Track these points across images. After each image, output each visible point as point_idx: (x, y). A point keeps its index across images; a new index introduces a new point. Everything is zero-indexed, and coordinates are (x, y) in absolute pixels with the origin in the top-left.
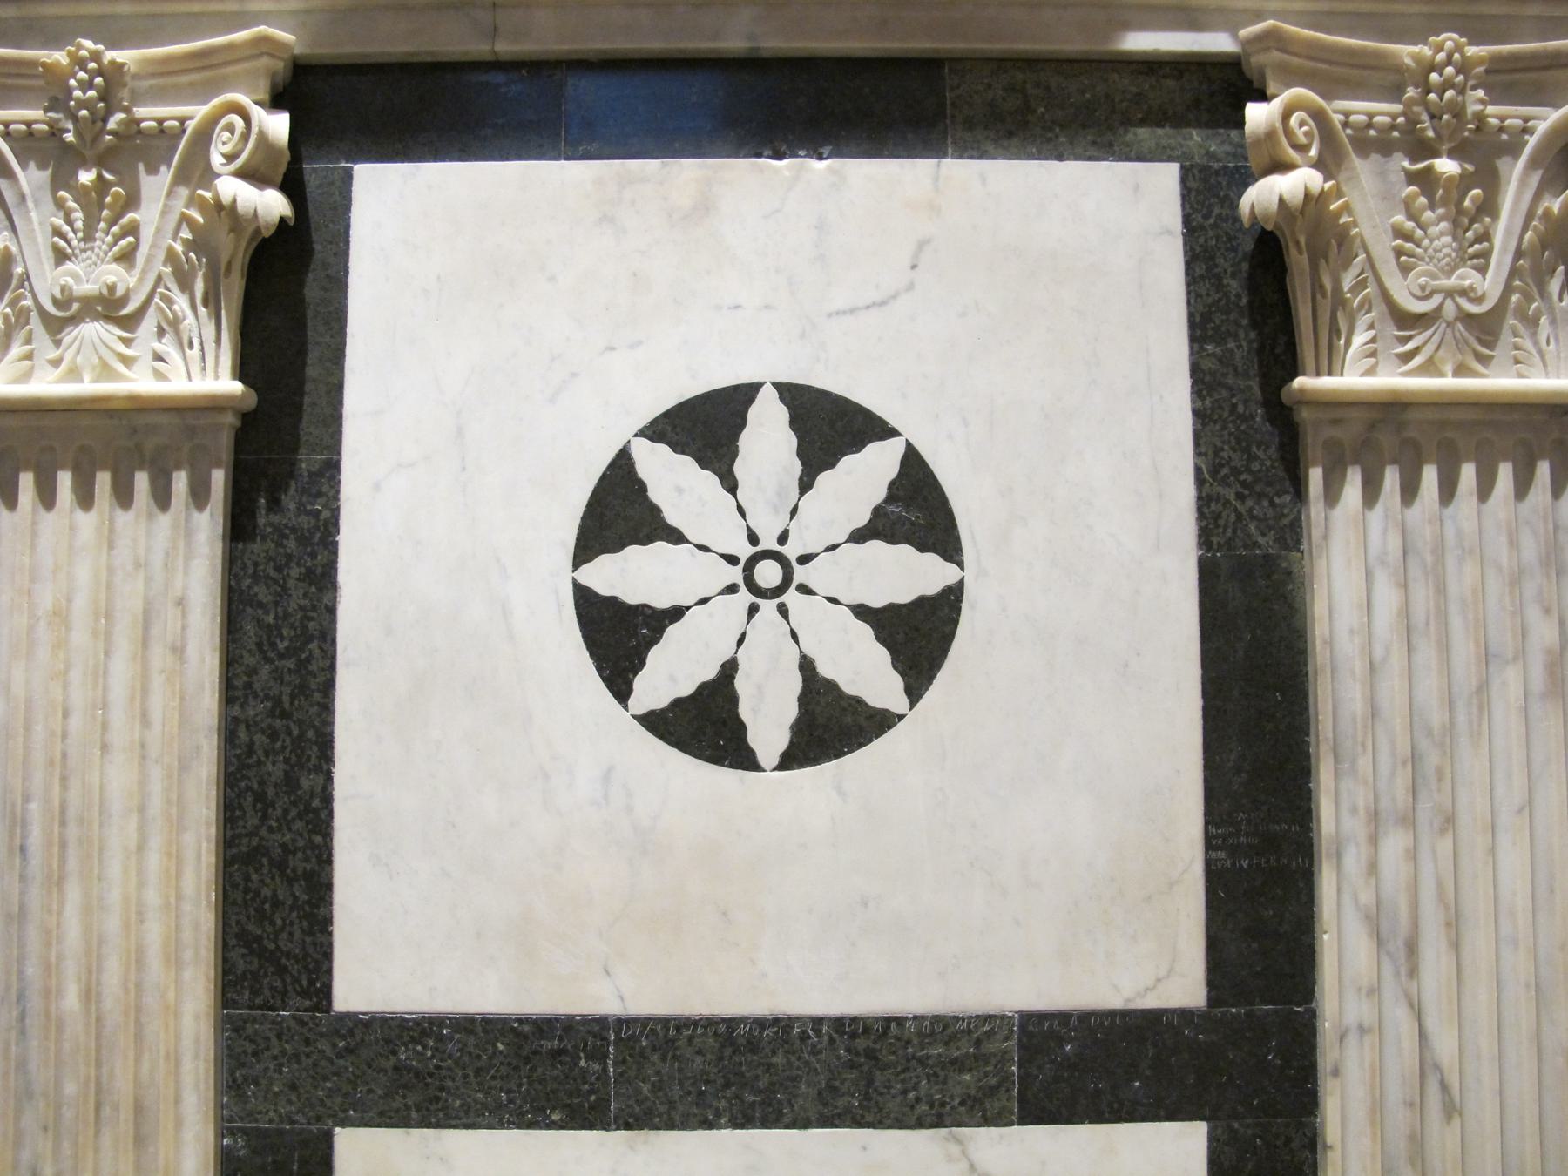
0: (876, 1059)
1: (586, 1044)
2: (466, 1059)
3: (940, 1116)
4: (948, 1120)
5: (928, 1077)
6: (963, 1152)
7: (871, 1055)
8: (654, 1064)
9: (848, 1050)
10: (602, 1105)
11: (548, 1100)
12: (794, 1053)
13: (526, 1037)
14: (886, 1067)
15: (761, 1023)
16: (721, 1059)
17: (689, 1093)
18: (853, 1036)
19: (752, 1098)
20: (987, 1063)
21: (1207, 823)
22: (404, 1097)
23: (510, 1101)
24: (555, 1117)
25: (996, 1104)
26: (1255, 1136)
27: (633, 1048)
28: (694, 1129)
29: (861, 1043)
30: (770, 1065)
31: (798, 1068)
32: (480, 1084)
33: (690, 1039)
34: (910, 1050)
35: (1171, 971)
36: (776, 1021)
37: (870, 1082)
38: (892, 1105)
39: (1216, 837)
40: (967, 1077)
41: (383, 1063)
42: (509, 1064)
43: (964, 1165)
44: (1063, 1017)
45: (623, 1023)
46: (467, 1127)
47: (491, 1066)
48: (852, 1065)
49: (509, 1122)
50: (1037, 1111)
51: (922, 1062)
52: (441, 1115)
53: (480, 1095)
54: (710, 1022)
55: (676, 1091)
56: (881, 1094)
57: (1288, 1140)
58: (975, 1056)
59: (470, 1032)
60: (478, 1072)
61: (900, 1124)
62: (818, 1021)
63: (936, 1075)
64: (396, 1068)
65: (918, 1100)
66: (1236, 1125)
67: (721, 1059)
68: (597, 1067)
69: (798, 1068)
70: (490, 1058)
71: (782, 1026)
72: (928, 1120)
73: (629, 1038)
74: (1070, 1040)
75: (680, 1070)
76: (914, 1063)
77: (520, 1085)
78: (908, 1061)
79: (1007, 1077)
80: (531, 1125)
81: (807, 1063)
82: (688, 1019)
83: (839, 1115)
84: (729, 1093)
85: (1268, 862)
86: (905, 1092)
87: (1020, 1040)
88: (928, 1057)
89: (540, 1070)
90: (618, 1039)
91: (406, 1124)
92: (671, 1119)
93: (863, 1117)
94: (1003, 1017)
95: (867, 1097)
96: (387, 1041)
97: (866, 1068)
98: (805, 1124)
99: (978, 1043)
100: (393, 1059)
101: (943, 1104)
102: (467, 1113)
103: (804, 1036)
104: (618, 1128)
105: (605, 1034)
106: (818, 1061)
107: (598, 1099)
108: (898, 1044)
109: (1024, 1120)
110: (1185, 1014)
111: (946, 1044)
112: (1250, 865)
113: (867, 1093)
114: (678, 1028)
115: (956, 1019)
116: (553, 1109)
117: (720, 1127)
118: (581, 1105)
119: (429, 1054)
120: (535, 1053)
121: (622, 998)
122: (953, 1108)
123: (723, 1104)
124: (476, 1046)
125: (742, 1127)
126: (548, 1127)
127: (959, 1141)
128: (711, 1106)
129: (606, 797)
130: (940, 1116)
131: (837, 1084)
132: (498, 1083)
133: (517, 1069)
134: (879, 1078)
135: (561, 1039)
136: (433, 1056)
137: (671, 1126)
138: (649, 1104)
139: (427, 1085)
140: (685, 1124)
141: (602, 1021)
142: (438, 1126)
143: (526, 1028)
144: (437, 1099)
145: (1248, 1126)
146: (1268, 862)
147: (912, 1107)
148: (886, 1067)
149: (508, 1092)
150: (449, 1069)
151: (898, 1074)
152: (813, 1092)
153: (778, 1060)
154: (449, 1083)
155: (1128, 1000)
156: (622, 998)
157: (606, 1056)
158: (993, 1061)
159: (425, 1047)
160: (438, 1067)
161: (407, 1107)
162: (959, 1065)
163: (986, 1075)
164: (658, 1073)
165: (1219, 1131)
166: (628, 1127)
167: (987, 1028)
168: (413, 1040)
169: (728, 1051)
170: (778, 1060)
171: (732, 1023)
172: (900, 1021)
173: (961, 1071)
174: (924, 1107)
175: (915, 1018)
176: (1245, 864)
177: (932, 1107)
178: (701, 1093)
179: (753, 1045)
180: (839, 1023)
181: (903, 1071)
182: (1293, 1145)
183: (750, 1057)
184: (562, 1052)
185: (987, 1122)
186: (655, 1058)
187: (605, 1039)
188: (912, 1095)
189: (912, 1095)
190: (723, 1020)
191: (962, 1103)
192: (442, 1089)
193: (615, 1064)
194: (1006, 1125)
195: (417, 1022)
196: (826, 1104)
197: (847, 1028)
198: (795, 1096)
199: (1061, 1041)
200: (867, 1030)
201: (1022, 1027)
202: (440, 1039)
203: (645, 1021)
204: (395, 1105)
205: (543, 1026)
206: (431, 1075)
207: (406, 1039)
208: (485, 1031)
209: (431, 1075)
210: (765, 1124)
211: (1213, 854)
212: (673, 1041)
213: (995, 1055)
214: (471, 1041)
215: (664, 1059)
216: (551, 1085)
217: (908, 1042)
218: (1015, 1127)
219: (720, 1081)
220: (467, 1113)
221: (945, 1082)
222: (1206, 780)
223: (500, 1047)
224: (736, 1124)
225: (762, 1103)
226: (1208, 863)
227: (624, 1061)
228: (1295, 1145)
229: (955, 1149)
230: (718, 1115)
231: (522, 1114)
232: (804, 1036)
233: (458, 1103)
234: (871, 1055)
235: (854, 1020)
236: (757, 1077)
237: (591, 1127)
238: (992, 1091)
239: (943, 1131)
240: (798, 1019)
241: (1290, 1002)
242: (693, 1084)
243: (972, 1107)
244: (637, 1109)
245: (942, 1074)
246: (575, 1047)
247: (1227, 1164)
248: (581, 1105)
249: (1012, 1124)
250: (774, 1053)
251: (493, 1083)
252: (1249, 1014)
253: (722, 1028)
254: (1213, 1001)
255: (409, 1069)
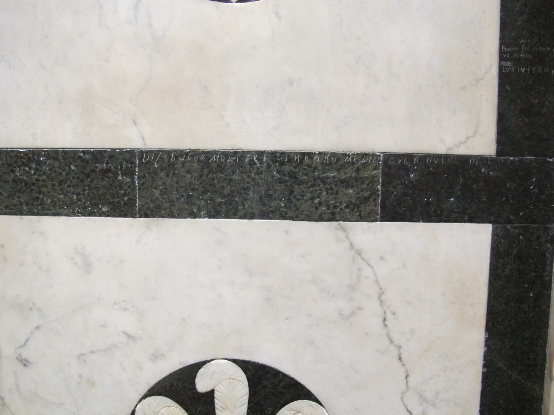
0: (296, 178)
1: (122, 166)
2: (54, 175)
3: (333, 214)
4: (338, 217)
5: (327, 189)
6: (346, 236)
7: (292, 175)
8: (162, 178)
9: (279, 172)
10: (131, 203)
11: (100, 199)
12: (246, 173)
13: (87, 162)
14: (302, 183)
15: (226, 154)
16: (201, 176)
17: (182, 196)
18: (282, 163)
19: (219, 200)
20: (363, 183)
21: (501, 45)
22: (19, 197)
23: (79, 200)
24: (104, 209)
25: (368, 208)
26: (520, 234)
27: (149, 169)
28: (185, 218)
29: (287, 168)
30: (231, 180)
31: (248, 183)
32: (61, 189)
33: (183, 163)
34: (316, 173)
35: (475, 132)
36: (235, 153)
37: (291, 192)
38: (305, 206)
39: (506, 53)
40: (351, 191)
41: (7, 178)
42: (78, 178)
43: (347, 244)
44: (410, 157)
45: (143, 153)
46: (54, 215)
47: (68, 179)
48: (281, 182)
49: (78, 212)
50: (393, 213)
51: (324, 181)
52: (40, 208)
53: (61, 196)
54: (195, 154)
55: (175, 195)
56: (298, 200)
57: (539, 237)
58: (356, 179)
59: (55, 159)
60: (61, 183)
61: (309, 218)
62: (260, 154)
63: (332, 189)
64: (14, 181)
65: (320, 204)
66: (509, 227)
67: (201, 176)
68: (128, 180)
69: (248, 183)
70: (67, 174)
71: (239, 156)
72: (327, 216)
73: (147, 163)
74: (414, 171)
75: (177, 182)
76: (318, 181)
77: (84, 190)
78: (315, 180)
79: (374, 192)
80: (91, 214)
81: (254, 179)
82: (182, 151)
83: (272, 211)
84: (206, 196)
85: (537, 70)
86: (312, 199)
87: (383, 170)
88: (327, 178)
89: (95, 181)
90: (141, 163)
91: (20, 213)
92: (172, 212)
93: (286, 213)
94: (373, 155)
95: (289, 201)
96: (9, 165)
97: (289, 183)
98: (252, 217)
99: (358, 170)
100: (12, 175)
101: (335, 207)
102: (54, 206)
103: (252, 163)
104: (140, 217)
105: (132, 160)
106: (260, 178)
107: (129, 199)
108: (309, 169)
109: (384, 219)
110: (483, 159)
111: (338, 170)
112: (526, 71)
113: (289, 199)
114: (176, 157)
115: (345, 155)
116: (103, 205)
117: (200, 217)
118: (119, 202)
119: (33, 172)
120: (92, 171)
121: (143, 139)
122: (341, 209)
123: (202, 203)
124: (59, 167)
125: (214, 217)
126: (100, 215)
127: (344, 229)
128: (195, 204)
129: (136, 18)
130: (333, 214)
131: (272, 192)
132: (72, 189)
133: (82, 181)
134: (297, 189)
135: (107, 163)
136: (35, 174)
137: (171, 215)
138: (158, 202)
139: (32, 190)
140: (180, 215)
141: (131, 152)
142: (38, 214)
143: (87, 156)
144: (38, 198)
145: (516, 228)
146: (537, 70)
147: (317, 208)
148: (302, 183)
149: (78, 194)
150: (44, 181)
151: (309, 188)
152: (257, 197)
153: (236, 177)
154: (44, 189)
155: (449, 149)
156: (143, 139)
157: (133, 173)
158: (367, 182)
159: (30, 168)
160: (38, 180)
161: (21, 204)
162: (346, 183)
163: (362, 190)
164: (164, 184)
165: (499, 230)
166: (146, 216)
167: (363, 161)
168: (24, 164)
169: (206, 171)
170: (236, 177)
171: (208, 154)
172: (310, 155)
173: (347, 187)
174: (324, 208)
175: (320, 154)
176: (523, 70)
177: (328, 209)
178: (189, 196)
179: (221, 168)
180: (274, 155)
181: (312, 186)
182: (541, 240)
183: (219, 175)
184: (108, 170)
185: (361, 219)
186: (162, 174)
187: (133, 163)
188: (317, 201)
189: (317, 201)
190: (203, 152)
191: (347, 207)
192: (40, 193)
193: (139, 178)
194: (373, 221)
195: (26, 154)
196: (264, 205)
197: (278, 158)
198: (246, 200)
199: (408, 171)
200: (290, 160)
201: (385, 162)
202: (39, 163)
203: (157, 153)
204: (14, 202)
205: (98, 155)
206: (33, 184)
207: (20, 163)
208: (65, 159)
209: (33, 184)
210: (227, 216)
211: (504, 63)
212: (173, 165)
213: (367, 178)
214: (56, 165)
215: (167, 175)
216: (102, 191)
217: (316, 168)
218: (379, 222)
219: (201, 189)
220: (54, 206)
221: (337, 194)
222: (501, 18)
223: (73, 168)
224: (210, 215)
225: (226, 203)
226: (501, 68)
227: (144, 177)
228: (542, 240)
229: (342, 234)
230: (199, 210)
231: (85, 208)
232: (252, 163)
233: (49, 201)
234: (292, 175)
235: (283, 153)
236: (223, 187)
237: (125, 216)
238: (367, 199)
239: (335, 223)
240: (249, 152)
241: (545, 156)
242: (186, 190)
243: (353, 210)
244: (152, 205)
245: (335, 188)
246: (116, 168)
247: (502, 250)
248: (119, 202)
249: (376, 220)
250: (234, 172)
251: (69, 189)
252: (520, 161)
253: (203, 157)
254: (500, 152)
255: (21, 181)
